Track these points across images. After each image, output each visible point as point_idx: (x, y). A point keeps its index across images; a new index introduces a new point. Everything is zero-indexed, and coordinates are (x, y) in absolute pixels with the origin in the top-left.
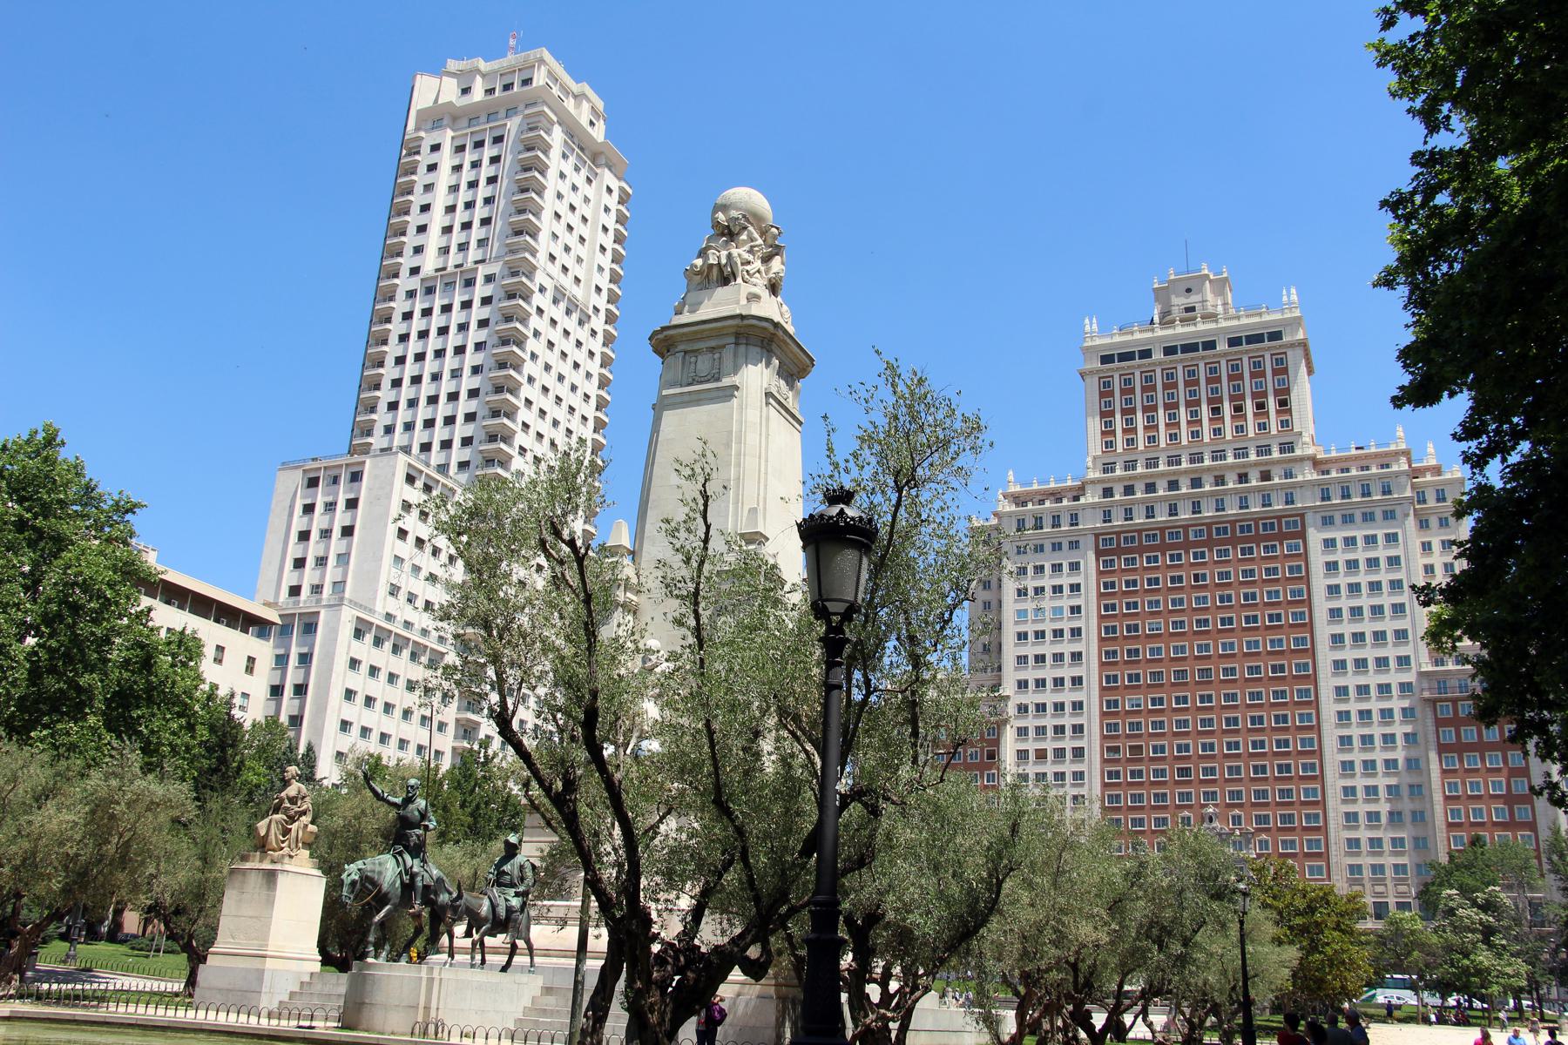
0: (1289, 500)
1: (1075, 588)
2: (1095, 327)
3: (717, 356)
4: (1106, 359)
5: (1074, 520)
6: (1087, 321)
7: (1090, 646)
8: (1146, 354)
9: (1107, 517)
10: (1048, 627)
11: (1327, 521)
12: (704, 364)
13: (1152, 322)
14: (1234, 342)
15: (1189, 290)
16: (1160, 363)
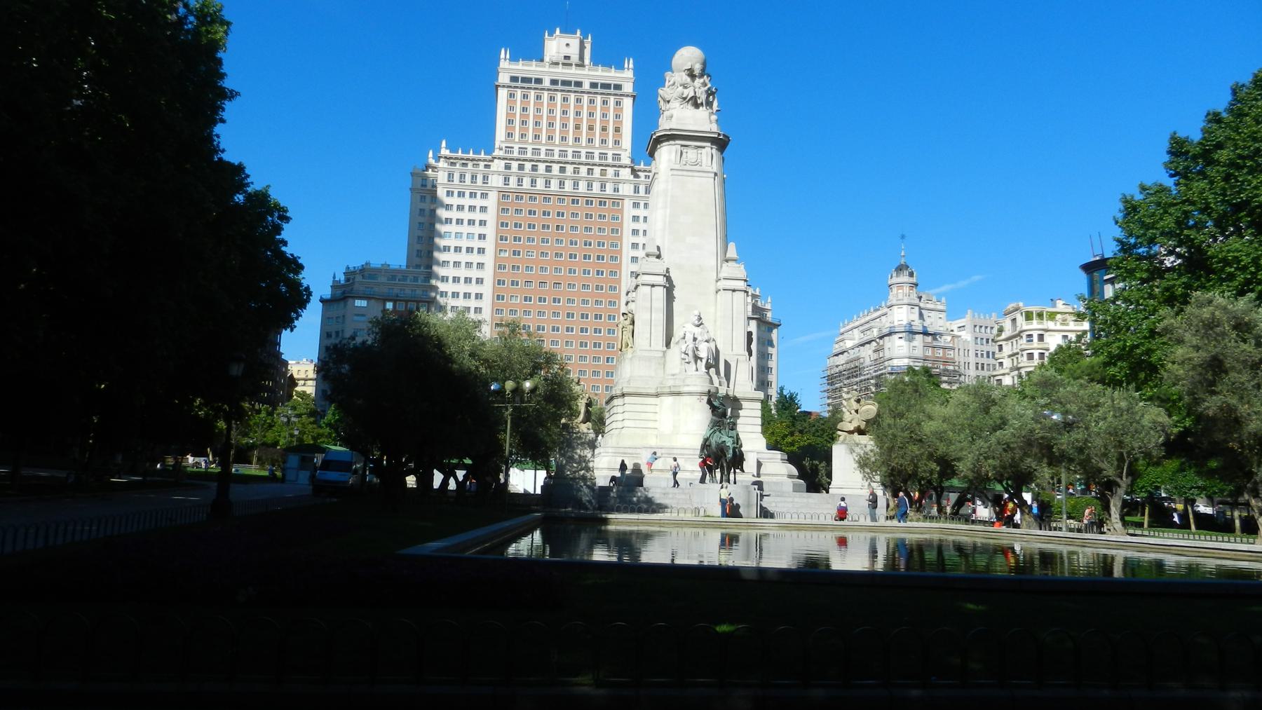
0: (616, 190)
1: (483, 223)
2: (508, 56)
3: (699, 152)
4: (514, 79)
5: (485, 178)
6: (503, 51)
7: (489, 259)
8: (539, 81)
9: (506, 180)
10: (464, 244)
11: (636, 205)
12: (691, 154)
13: (542, 60)
14: (594, 85)
15: (568, 45)
16: (548, 90)
